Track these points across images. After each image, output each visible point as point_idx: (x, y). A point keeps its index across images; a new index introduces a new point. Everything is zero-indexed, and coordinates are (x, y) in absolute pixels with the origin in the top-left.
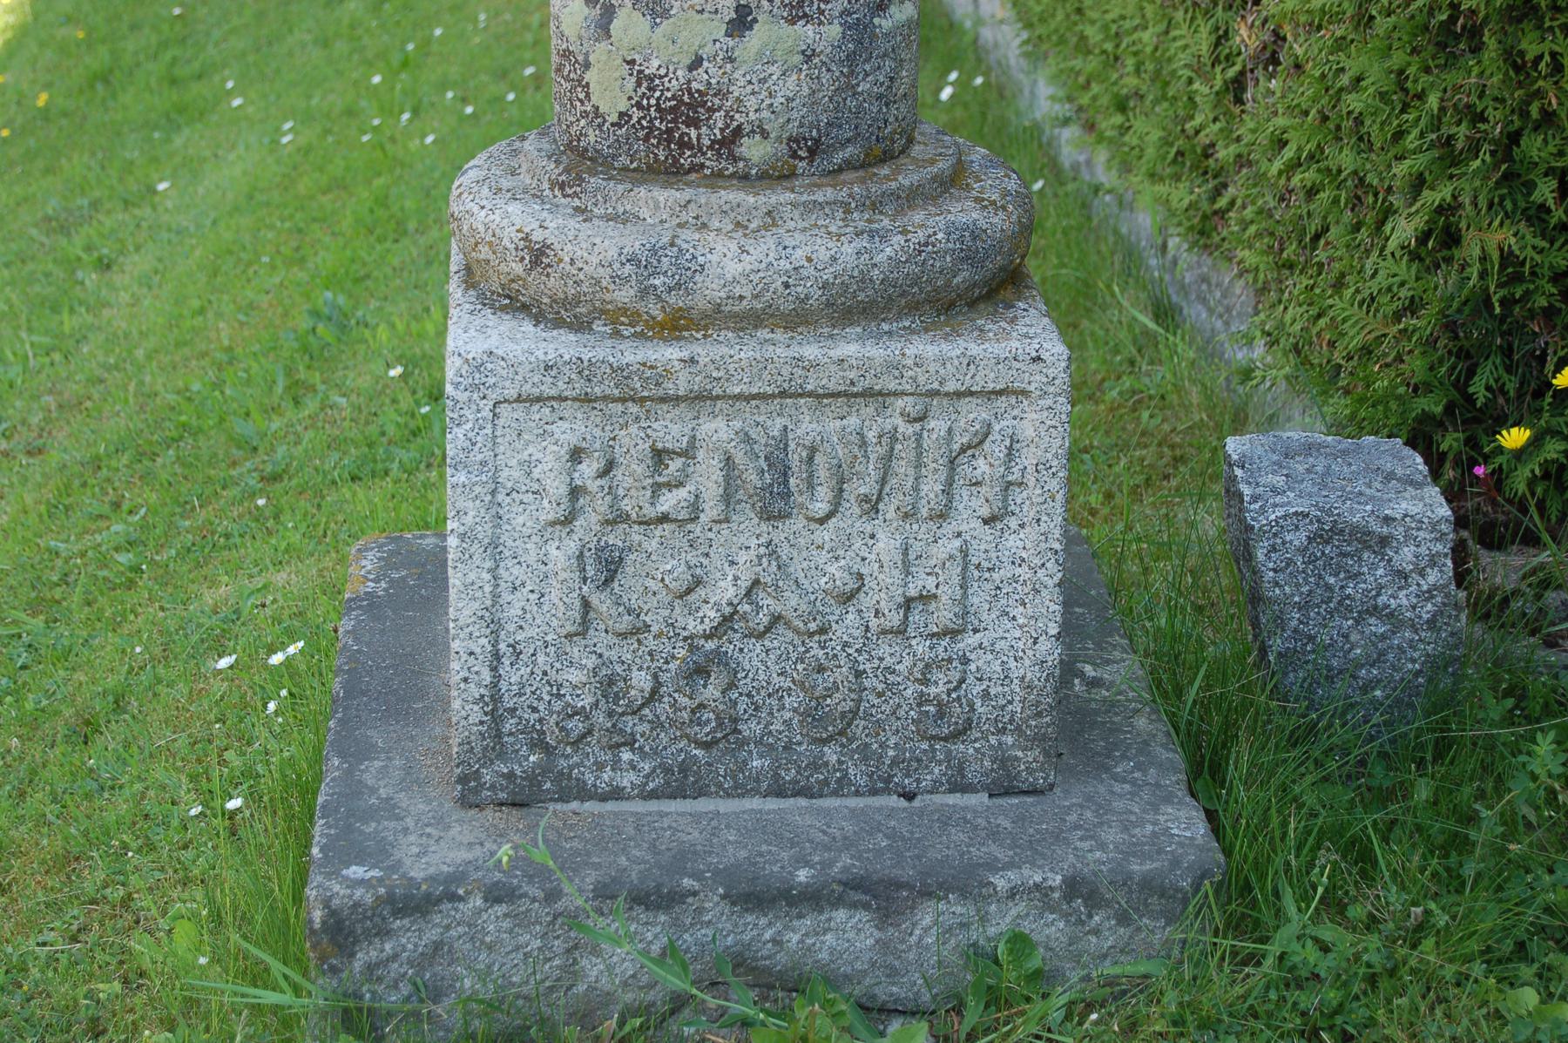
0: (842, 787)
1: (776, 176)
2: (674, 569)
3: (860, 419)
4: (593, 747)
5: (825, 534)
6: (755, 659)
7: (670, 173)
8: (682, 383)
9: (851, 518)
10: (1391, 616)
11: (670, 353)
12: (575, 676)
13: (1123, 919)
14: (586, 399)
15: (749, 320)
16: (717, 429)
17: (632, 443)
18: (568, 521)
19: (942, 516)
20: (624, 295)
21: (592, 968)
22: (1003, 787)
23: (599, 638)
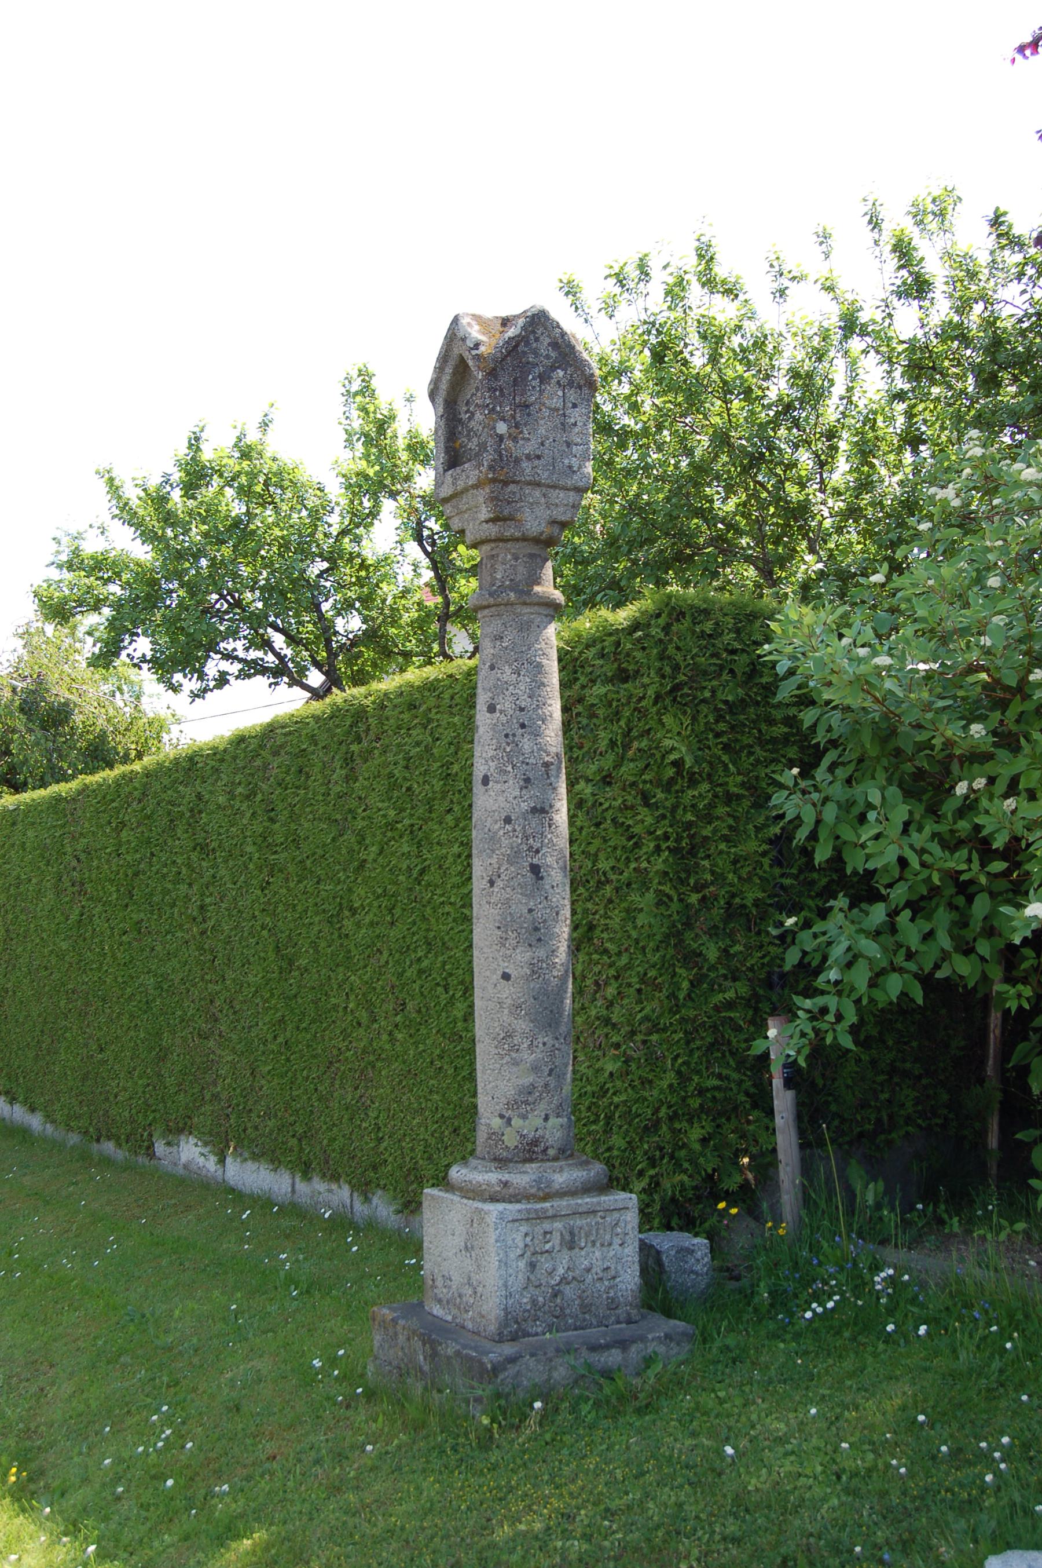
0: (591, 1326)
1: (556, 1159)
2: (548, 1266)
3: (591, 1220)
4: (530, 1323)
5: (583, 1253)
6: (568, 1291)
7: (531, 1160)
8: (550, 1213)
9: (589, 1249)
10: (697, 1273)
11: (548, 1205)
12: (525, 1300)
13: (678, 1344)
14: (528, 1219)
15: (562, 1194)
16: (558, 1225)
17: (539, 1230)
18: (522, 1255)
19: (610, 1244)
20: (533, 1191)
21: (555, 1374)
22: (629, 1322)
23: (531, 1289)
